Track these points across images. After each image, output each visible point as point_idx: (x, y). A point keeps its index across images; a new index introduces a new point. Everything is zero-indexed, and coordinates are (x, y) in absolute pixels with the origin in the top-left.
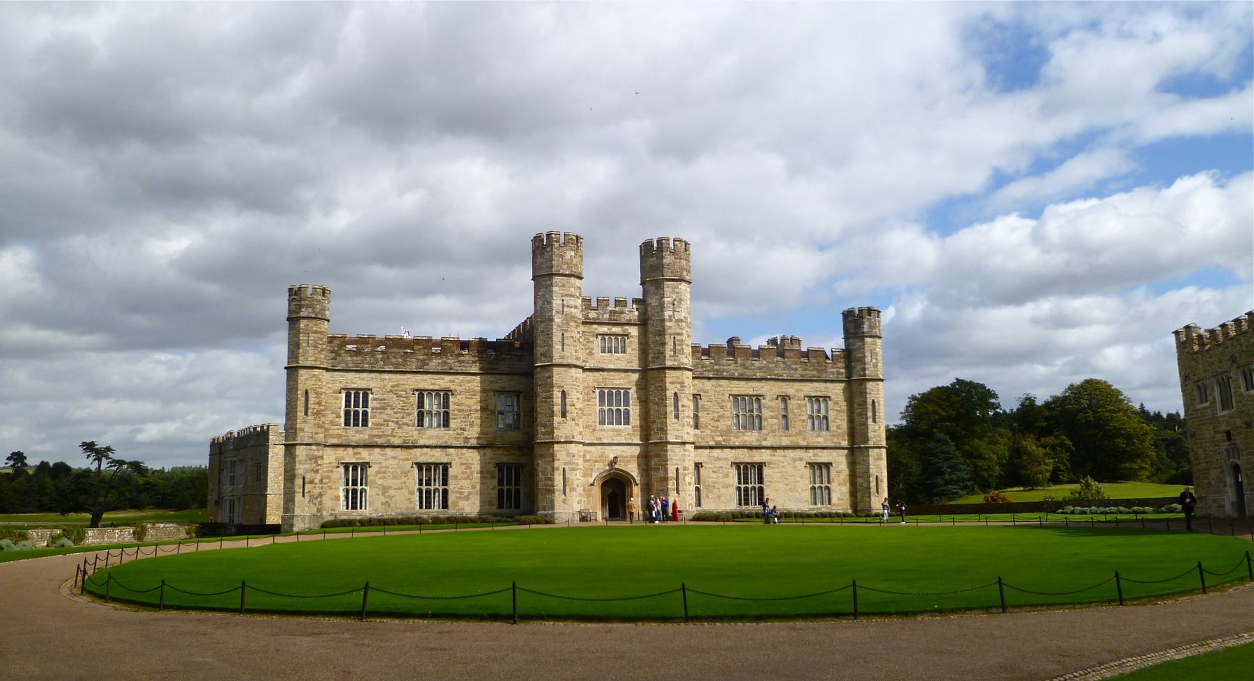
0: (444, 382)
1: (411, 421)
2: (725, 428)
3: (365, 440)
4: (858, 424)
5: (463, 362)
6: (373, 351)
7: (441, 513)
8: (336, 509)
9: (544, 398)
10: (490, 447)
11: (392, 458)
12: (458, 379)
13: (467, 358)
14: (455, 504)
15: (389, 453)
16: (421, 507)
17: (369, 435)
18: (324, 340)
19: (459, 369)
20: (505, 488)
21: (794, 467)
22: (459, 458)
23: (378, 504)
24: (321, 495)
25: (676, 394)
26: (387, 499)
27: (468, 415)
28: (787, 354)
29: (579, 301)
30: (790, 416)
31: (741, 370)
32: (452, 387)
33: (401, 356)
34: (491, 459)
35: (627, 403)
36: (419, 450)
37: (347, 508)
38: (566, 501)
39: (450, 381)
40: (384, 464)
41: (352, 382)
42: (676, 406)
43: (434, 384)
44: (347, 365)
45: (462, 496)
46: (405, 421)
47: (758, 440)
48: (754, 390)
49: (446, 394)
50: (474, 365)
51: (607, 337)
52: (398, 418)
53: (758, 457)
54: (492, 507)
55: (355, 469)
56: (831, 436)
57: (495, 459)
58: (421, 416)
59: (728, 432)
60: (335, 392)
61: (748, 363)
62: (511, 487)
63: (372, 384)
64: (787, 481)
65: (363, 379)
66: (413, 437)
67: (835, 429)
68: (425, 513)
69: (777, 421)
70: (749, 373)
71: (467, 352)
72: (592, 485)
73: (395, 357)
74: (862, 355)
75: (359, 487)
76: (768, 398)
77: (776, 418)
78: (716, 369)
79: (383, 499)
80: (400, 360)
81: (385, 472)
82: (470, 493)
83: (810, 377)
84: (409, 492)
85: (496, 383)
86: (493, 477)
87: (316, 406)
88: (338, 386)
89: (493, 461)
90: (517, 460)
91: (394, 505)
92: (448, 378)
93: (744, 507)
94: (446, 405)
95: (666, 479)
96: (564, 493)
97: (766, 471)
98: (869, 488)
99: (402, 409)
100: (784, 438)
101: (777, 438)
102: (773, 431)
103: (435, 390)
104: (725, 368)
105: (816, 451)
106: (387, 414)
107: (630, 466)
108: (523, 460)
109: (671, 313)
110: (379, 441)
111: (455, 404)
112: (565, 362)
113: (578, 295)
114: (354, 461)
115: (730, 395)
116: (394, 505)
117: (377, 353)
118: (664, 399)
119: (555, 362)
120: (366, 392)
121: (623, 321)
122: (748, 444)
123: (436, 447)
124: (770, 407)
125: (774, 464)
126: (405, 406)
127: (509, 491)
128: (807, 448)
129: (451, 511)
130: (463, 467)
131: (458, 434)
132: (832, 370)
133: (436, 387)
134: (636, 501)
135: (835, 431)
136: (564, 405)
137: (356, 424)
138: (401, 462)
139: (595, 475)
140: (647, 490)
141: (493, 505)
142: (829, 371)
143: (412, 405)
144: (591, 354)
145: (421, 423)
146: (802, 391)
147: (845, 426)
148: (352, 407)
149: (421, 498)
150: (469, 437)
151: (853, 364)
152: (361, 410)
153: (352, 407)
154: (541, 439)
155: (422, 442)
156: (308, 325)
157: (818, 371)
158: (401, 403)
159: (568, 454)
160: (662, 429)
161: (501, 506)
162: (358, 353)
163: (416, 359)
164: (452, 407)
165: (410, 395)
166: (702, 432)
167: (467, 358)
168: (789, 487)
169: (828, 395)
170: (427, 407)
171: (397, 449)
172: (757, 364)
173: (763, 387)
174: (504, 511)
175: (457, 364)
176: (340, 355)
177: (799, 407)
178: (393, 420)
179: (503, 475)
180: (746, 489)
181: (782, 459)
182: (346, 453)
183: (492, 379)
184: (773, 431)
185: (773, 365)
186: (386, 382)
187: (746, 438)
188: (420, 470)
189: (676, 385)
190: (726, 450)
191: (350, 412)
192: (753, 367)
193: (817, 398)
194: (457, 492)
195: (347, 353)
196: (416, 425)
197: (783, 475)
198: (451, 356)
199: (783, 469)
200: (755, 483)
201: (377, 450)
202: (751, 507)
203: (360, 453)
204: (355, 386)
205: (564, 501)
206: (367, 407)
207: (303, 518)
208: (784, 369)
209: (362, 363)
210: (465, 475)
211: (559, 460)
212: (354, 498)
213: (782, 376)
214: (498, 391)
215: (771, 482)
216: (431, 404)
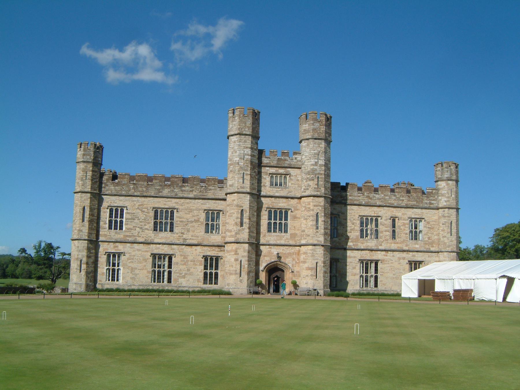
1: (150, 227)
2: (355, 237)
3: (122, 238)
4: (442, 236)
5: (184, 191)
6: (128, 183)
7: (167, 286)
8: (102, 280)
9: (231, 213)
11: (137, 250)
12: (180, 201)
13: (187, 188)
14: (175, 280)
15: (136, 247)
16: (155, 282)
18: (97, 176)
19: (181, 195)
20: (208, 271)
21: (399, 263)
22: (179, 251)
23: (128, 279)
26: (134, 276)
27: (186, 225)
28: (396, 190)
29: (257, 152)
31: (366, 200)
32: (177, 207)
33: (145, 187)
34: (200, 253)
35: (286, 219)
36: (154, 245)
38: (242, 281)
39: (177, 203)
40: (132, 254)
41: (114, 202)
43: (165, 204)
44: (111, 191)
45: (181, 275)
46: (146, 227)
47: (376, 246)
48: (374, 213)
50: (191, 192)
51: (274, 176)
52: (142, 225)
54: (200, 283)
55: (114, 256)
56: (424, 244)
57: (202, 253)
58: (155, 224)
61: (371, 195)
62: (212, 271)
64: (394, 272)
65: (121, 200)
66: (151, 237)
67: (427, 239)
68: (156, 286)
69: (389, 233)
70: (372, 202)
71: (187, 185)
74: (446, 192)
75: (116, 268)
76: (384, 218)
77: (388, 231)
78: (350, 199)
79: (131, 275)
80: (144, 189)
81: (133, 259)
82: (186, 274)
83: (412, 205)
84: (147, 271)
85: (205, 204)
86: (200, 265)
87: (91, 217)
89: (202, 255)
90: (217, 254)
91: (138, 280)
92: (174, 200)
93: (364, 288)
94: (172, 218)
97: (380, 265)
99: (145, 220)
100: (393, 245)
101: (389, 245)
102: (387, 240)
103: (165, 208)
104: (356, 198)
105: (414, 253)
106: (135, 223)
107: (287, 260)
108: (220, 254)
109: (316, 160)
110: (130, 239)
111: (178, 217)
113: (255, 148)
114: (114, 251)
116: (138, 280)
117: (130, 184)
119: (238, 190)
121: (286, 165)
122: (369, 248)
123: (165, 244)
124: (386, 225)
125: (386, 261)
126: (146, 218)
127: (211, 274)
129: (173, 286)
131: (179, 236)
132: (426, 201)
135: (428, 241)
137: (116, 228)
142: (424, 202)
143: (151, 218)
146: (406, 214)
148: (114, 218)
150: (186, 238)
151: (440, 198)
152: (119, 220)
153: (114, 218)
155: (156, 241)
156: (87, 166)
157: (417, 202)
158: (144, 216)
161: (205, 283)
162: (118, 184)
163: (155, 189)
165: (149, 211)
166: (339, 239)
168: (394, 276)
169: (423, 217)
171: (141, 245)
172: (377, 196)
173: (380, 211)
174: (208, 287)
175: (180, 192)
176: (107, 185)
177: (404, 225)
178: (138, 226)
179: (207, 263)
180: (366, 277)
182: (109, 246)
183: (202, 202)
184: (387, 240)
185: (388, 197)
186: (135, 203)
187: (368, 244)
189: (317, 208)
191: (112, 221)
192: (375, 198)
194: (177, 273)
195: (111, 185)
196: (153, 229)
197: (391, 269)
198: (177, 187)
199: (392, 265)
200: (363, 273)
201: (128, 245)
202: (369, 288)
203: (117, 247)
204: (116, 205)
205: (241, 281)
206: (123, 218)
207: (81, 285)
209: (121, 190)
211: (238, 254)
212: (113, 274)
213: (393, 204)
214: (205, 210)
215: (384, 273)
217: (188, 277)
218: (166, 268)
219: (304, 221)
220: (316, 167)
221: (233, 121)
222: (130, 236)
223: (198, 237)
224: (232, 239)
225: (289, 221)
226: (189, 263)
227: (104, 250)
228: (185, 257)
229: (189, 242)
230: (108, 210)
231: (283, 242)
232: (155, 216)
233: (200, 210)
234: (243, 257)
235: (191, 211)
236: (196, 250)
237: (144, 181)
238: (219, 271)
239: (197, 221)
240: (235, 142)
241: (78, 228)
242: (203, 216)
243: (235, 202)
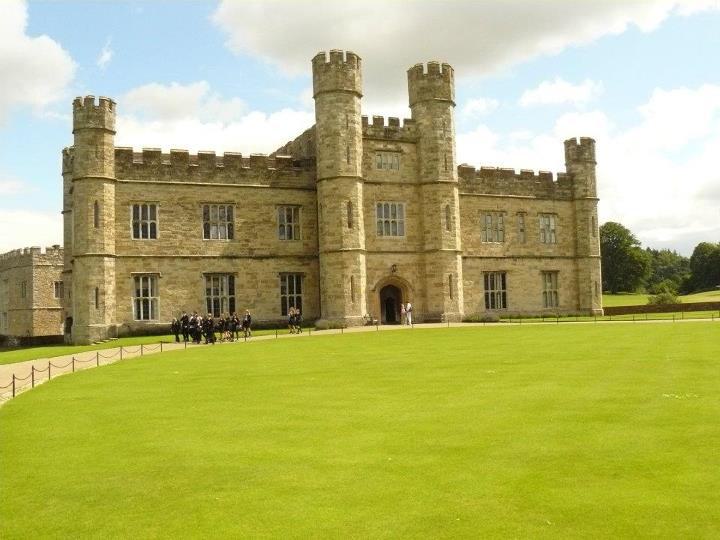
0: (229, 195)
10: (272, 257)
14: (241, 311)
17: (158, 247)
20: (288, 296)
27: (253, 227)
32: (236, 201)
35: (402, 215)
37: (139, 318)
40: (175, 274)
43: (219, 197)
51: (383, 153)
53: (507, 265)
55: (145, 280)
59: (477, 245)
61: (493, 183)
63: (160, 196)
72: (374, 291)
73: (181, 171)
75: (150, 298)
81: (175, 283)
82: (255, 301)
86: (277, 286)
88: (126, 198)
96: (353, 300)
97: (508, 278)
98: (590, 292)
100: (522, 250)
108: (304, 269)
110: (170, 253)
115: (480, 211)
121: (396, 138)
124: (511, 222)
127: (291, 299)
128: (540, 258)
130: (249, 276)
133: (221, 200)
137: (145, 236)
138: (191, 273)
139: (376, 282)
141: (277, 312)
145: (207, 235)
147: (570, 239)
149: (209, 306)
151: (576, 186)
160: (436, 238)
164: (236, 220)
167: (250, 173)
177: (534, 222)
180: (493, 294)
181: (522, 268)
190: (478, 260)
201: (166, 261)
204: (142, 198)
205: (353, 307)
208: (522, 189)
210: (250, 285)
217: (259, 307)
218: (226, 293)
219: (429, 218)
220: (440, 142)
221: (325, 72)
222: (168, 248)
223: (269, 245)
224: (336, 246)
225: (404, 219)
226: (260, 284)
227: (129, 270)
228: (253, 276)
229: (257, 253)
230: (131, 208)
231: (398, 249)
232: (205, 214)
233: (270, 204)
235: (257, 206)
236: (268, 265)
238: (302, 295)
239: (266, 222)
240: (331, 102)
241: (90, 238)
243: (337, 192)
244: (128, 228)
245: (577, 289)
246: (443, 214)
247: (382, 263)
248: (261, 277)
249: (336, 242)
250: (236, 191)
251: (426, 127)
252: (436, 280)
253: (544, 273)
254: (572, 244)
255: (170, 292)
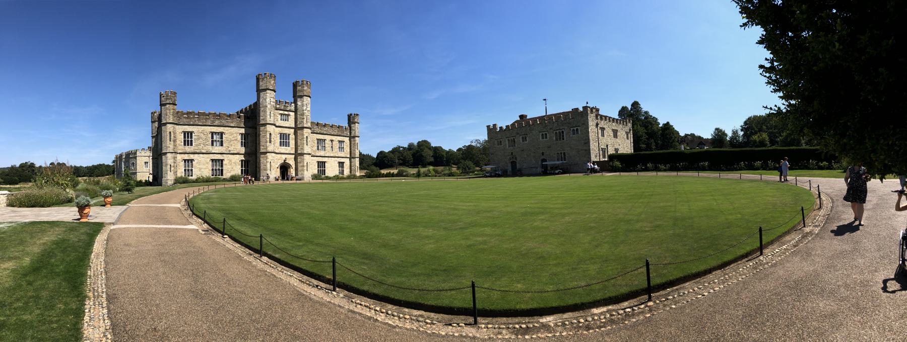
13: (229, 120)
19: (227, 125)
24: (177, 172)
25: (307, 137)
30: (333, 147)
31: (320, 131)
32: (224, 131)
35: (289, 140)
40: (200, 159)
42: (307, 141)
49: (221, 134)
55: (188, 162)
58: (212, 142)
60: (180, 133)
70: (322, 132)
82: (231, 170)
86: (239, 165)
88: (181, 131)
94: (222, 138)
95: (304, 166)
96: (270, 170)
97: (326, 164)
108: (250, 159)
110: (198, 151)
112: (271, 122)
114: (188, 158)
118: (303, 138)
119: (268, 122)
120: (191, 133)
121: (288, 109)
128: (338, 157)
133: (218, 131)
134: (292, 172)
136: (270, 139)
139: (279, 164)
140: (296, 169)
144: (277, 120)
145: (212, 145)
147: (349, 151)
152: (190, 139)
154: (262, 151)
155: (213, 152)
159: (272, 157)
160: (302, 149)
162: (188, 118)
170: (215, 139)
188: (213, 162)
193: (341, 141)
201: (196, 155)
207: (171, 180)
216: (216, 137)
220: (305, 112)
229: (232, 152)
231: (287, 152)
234: (271, 160)
235: (232, 134)
237: (203, 116)
242: (239, 137)
244: (182, 142)
245: (351, 169)
246: (305, 139)
247: (281, 157)
248: (233, 161)
249: (265, 149)
250: (222, 128)
251: (300, 105)
252: (301, 164)
253: (339, 163)
254: (349, 152)
255: (198, 166)
